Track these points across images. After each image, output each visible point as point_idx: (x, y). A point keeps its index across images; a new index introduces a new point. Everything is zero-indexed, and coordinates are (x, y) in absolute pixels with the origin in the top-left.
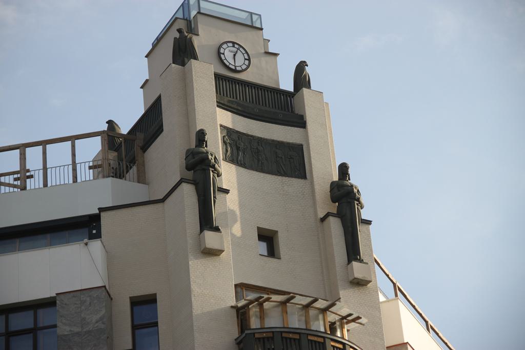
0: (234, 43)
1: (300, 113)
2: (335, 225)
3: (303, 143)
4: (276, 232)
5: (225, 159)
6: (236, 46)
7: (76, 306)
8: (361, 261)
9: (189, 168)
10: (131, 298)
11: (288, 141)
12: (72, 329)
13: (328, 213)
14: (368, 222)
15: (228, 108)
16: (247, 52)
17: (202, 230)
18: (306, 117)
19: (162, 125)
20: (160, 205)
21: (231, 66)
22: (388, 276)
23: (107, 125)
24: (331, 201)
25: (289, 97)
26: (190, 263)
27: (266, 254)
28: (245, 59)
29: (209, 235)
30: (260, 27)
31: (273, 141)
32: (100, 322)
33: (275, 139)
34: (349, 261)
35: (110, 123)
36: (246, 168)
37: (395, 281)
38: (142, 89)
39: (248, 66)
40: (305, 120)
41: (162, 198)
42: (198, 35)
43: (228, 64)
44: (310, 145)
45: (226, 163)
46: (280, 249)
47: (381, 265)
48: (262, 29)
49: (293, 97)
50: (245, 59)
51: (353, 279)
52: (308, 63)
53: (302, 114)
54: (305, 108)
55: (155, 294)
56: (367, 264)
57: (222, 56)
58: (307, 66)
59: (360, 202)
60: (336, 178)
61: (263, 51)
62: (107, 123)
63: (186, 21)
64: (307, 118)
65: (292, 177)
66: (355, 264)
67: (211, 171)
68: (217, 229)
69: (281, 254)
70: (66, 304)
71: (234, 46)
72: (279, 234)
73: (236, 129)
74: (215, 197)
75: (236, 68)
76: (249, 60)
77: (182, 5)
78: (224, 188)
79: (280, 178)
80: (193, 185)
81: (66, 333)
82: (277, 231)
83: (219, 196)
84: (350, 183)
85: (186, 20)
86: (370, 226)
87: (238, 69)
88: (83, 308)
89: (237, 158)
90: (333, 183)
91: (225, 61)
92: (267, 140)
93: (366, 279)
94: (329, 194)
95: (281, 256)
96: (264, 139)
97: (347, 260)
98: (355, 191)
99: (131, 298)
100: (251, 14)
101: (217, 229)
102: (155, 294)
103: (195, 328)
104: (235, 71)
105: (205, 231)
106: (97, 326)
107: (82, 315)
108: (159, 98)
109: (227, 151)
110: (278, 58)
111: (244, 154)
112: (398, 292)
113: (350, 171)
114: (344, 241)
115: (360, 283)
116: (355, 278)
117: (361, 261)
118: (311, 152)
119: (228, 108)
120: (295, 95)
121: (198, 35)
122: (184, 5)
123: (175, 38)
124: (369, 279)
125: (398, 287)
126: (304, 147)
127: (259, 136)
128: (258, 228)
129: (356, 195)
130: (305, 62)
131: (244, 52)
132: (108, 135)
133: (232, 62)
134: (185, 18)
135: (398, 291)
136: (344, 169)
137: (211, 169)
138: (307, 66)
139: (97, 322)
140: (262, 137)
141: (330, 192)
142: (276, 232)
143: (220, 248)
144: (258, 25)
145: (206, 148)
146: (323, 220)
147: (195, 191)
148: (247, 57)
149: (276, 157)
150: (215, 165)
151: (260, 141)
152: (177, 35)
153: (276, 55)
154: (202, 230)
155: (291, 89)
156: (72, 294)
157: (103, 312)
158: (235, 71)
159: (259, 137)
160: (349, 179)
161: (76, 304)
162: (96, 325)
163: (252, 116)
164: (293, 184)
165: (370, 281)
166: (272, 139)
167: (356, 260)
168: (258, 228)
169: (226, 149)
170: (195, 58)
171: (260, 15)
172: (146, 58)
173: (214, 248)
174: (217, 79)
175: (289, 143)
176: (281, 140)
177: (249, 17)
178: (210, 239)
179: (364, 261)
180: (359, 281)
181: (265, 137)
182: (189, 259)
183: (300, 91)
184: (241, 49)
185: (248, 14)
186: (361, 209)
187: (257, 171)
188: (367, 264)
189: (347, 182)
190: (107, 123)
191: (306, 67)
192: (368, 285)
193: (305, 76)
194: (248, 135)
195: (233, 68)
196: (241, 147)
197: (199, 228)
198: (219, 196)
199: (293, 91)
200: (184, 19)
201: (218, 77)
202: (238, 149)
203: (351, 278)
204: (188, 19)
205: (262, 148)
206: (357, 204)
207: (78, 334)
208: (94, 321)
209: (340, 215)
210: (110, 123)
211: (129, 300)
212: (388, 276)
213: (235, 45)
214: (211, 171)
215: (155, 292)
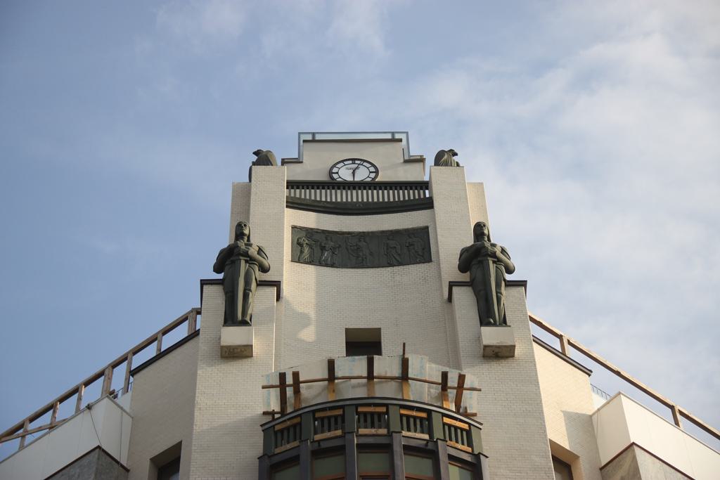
2: (465, 299)
9: (218, 269)
14: (523, 284)
15: (309, 208)
16: (373, 165)
22: (618, 373)
24: (459, 272)
26: (199, 372)
31: (383, 232)
37: (671, 403)
47: (622, 373)
56: (510, 326)
58: (456, 154)
61: (402, 161)
92: (372, 233)
96: (368, 233)
112: (679, 416)
114: (477, 311)
115: (500, 354)
119: (309, 208)
125: (681, 413)
126: (429, 229)
127: (361, 231)
131: (368, 165)
135: (679, 416)
136: (480, 231)
138: (456, 154)
149: (387, 249)
151: (362, 236)
156: (61, 473)
159: (360, 233)
163: (350, 212)
166: (381, 229)
167: (489, 324)
180: (497, 350)
181: (370, 230)
182: (199, 368)
184: (365, 164)
188: (510, 326)
191: (455, 158)
194: (343, 233)
196: (327, 246)
205: (365, 244)
212: (618, 373)
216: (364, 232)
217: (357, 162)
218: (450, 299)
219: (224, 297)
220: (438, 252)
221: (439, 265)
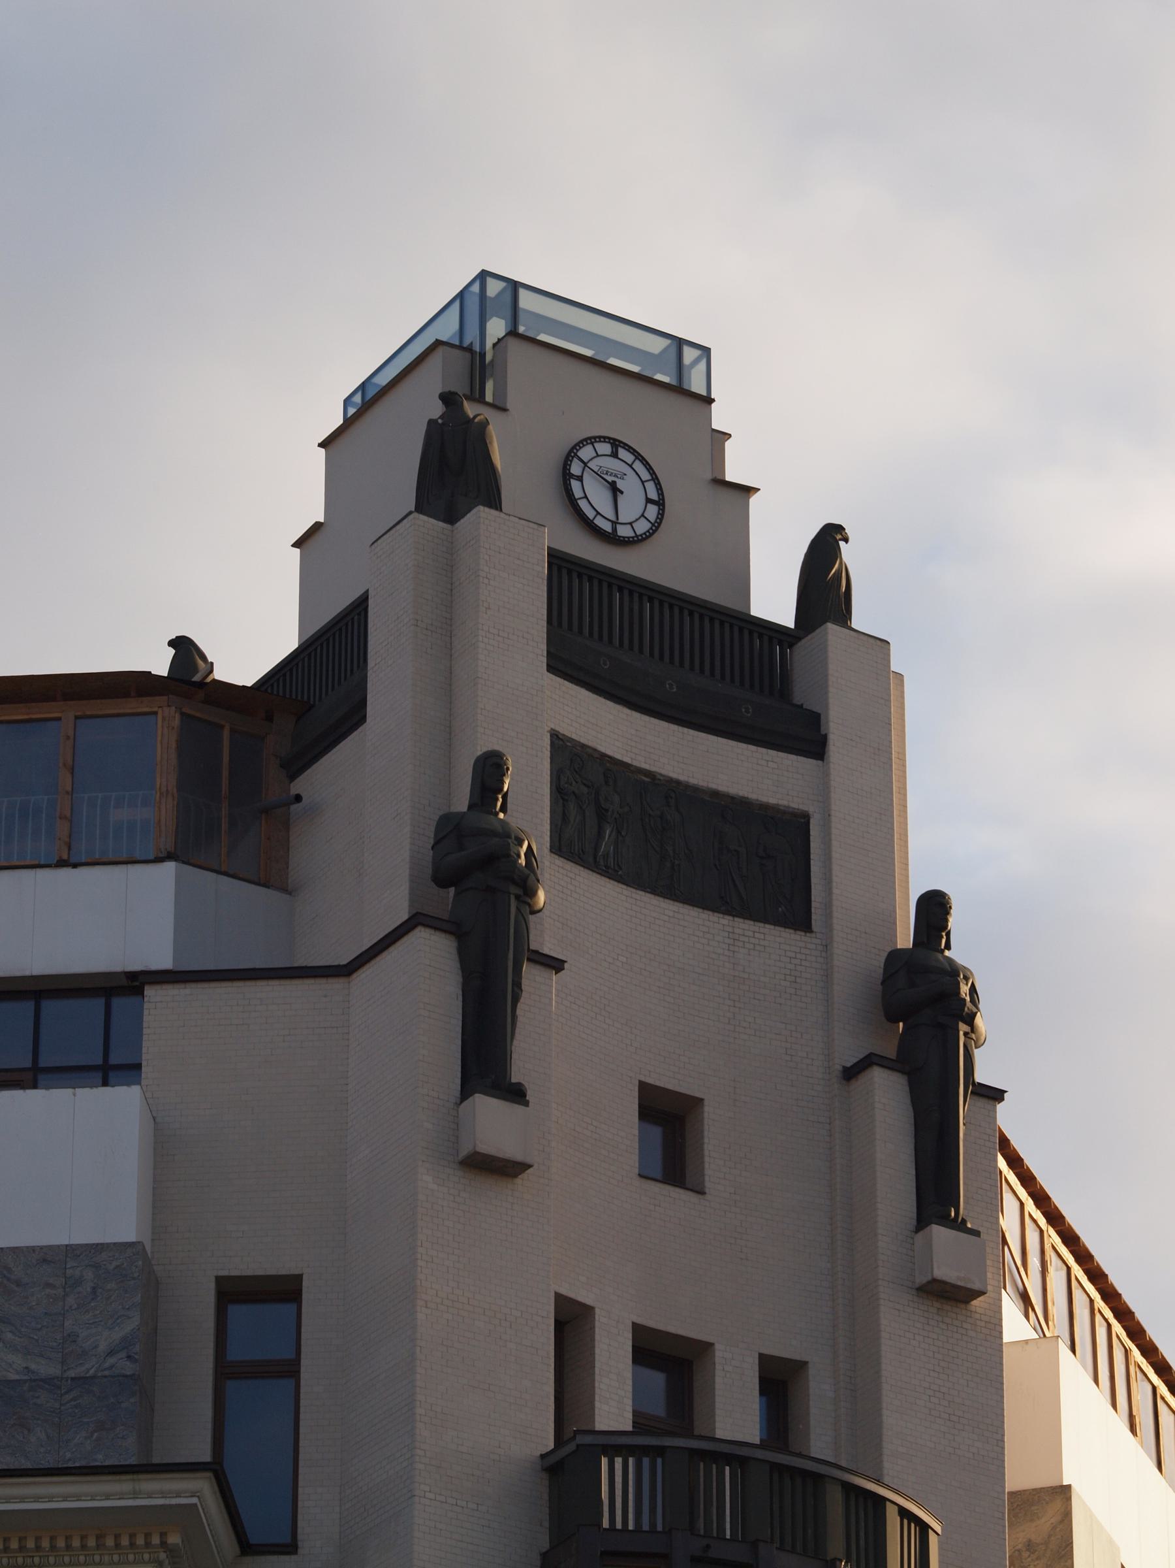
0: (616, 444)
1: (811, 705)
3: (811, 809)
4: (697, 1102)
5: (560, 847)
7: (48, 1291)
8: (959, 1225)
9: (442, 879)
10: (219, 1280)
11: (764, 799)
12: (33, 1366)
13: (871, 1054)
17: (466, 1092)
18: (827, 722)
19: (363, 703)
20: (334, 985)
21: (599, 522)
23: (172, 651)
25: (780, 643)
27: (659, 1177)
28: (649, 501)
30: (704, 393)
31: (716, 794)
32: (123, 1354)
33: (722, 788)
34: (922, 1222)
35: (183, 647)
36: (620, 880)
38: (298, 551)
39: (656, 526)
40: (823, 732)
41: (344, 962)
43: (590, 514)
44: (833, 819)
45: (559, 861)
46: (707, 1159)
48: (709, 400)
49: (791, 646)
50: (649, 501)
51: (929, 1282)
52: (849, 531)
53: (816, 709)
54: (827, 693)
55: (299, 1278)
56: (976, 1233)
57: (575, 484)
58: (846, 540)
59: (973, 1028)
60: (905, 938)
61: (709, 476)
62: (172, 643)
63: (468, 355)
64: (831, 724)
65: (765, 920)
66: (938, 1232)
67: (512, 898)
68: (517, 1094)
69: (707, 1178)
70: (18, 1283)
71: (615, 455)
72: (706, 1109)
73: (603, 750)
74: (517, 985)
75: (615, 530)
76: (660, 503)
77: (461, 295)
78: (546, 951)
79: (726, 920)
80: (448, 936)
81: (13, 1376)
82: (702, 1100)
83: (531, 975)
84: (949, 960)
85: (469, 349)
86: (1000, 1107)
87: (624, 532)
88: (71, 1301)
89: (596, 848)
90: (895, 957)
91: (583, 504)
92: (696, 789)
93: (969, 1286)
94: (880, 988)
95: (707, 1184)
96: (687, 786)
97: (915, 1216)
98: (965, 989)
99: (219, 1280)
100: (680, 343)
101: (517, 1094)
102: (299, 1278)
103: (419, 1411)
104: (611, 539)
105: (477, 1095)
106: (111, 1367)
107: (67, 1324)
108: (360, 607)
109: (565, 818)
110: (754, 500)
111: (619, 832)
113: (952, 922)
116: (934, 1281)
117: (959, 1225)
118: (835, 843)
120: (799, 639)
122: (467, 295)
123: (431, 423)
124: (976, 1286)
126: (812, 821)
127: (674, 776)
128: (640, 1082)
129: (965, 1004)
130: (839, 528)
131: (645, 475)
132: (183, 714)
133: (607, 510)
134: (466, 344)
137: (514, 890)
138: (846, 540)
139: (111, 1353)
140: (682, 778)
141: (883, 983)
142: (697, 1102)
143: (519, 1157)
144: (698, 387)
145: (501, 815)
146: (850, 1074)
147: (455, 956)
148: (653, 495)
150: (528, 877)
153: (748, 491)
154: (466, 1092)
155: (790, 622)
157: (133, 1323)
158: (611, 539)
159: (670, 780)
160: (948, 947)
161: (48, 1285)
162: (111, 1361)
165: (982, 1293)
166: (713, 786)
168: (640, 1082)
169: (564, 813)
170: (493, 500)
171: (706, 351)
172: (323, 451)
173: (501, 1155)
174: (555, 569)
175: (765, 807)
176: (741, 793)
177: (673, 350)
179: (969, 1225)
181: (693, 781)
183: (823, 627)
184: (638, 466)
185: (667, 342)
186: (976, 1048)
187: (654, 891)
188: (976, 1233)
189: (940, 956)
190: (172, 643)
191: (842, 544)
192: (974, 1303)
193: (838, 574)
195: (607, 527)
197: (458, 1081)
198: (531, 975)
199: (792, 625)
200: (460, 347)
201: (559, 563)
202: (601, 815)
203: (921, 1279)
204: (477, 348)
206: (966, 1034)
207: (49, 1383)
208: (103, 1346)
209: (903, 1063)
210: (183, 647)
211: (212, 1285)
214: (512, 898)
215: (297, 1272)
216: (678, 782)
217: (622, 453)
218: (850, 1074)
219: (461, 980)
220: (828, 906)
221: (827, 947)
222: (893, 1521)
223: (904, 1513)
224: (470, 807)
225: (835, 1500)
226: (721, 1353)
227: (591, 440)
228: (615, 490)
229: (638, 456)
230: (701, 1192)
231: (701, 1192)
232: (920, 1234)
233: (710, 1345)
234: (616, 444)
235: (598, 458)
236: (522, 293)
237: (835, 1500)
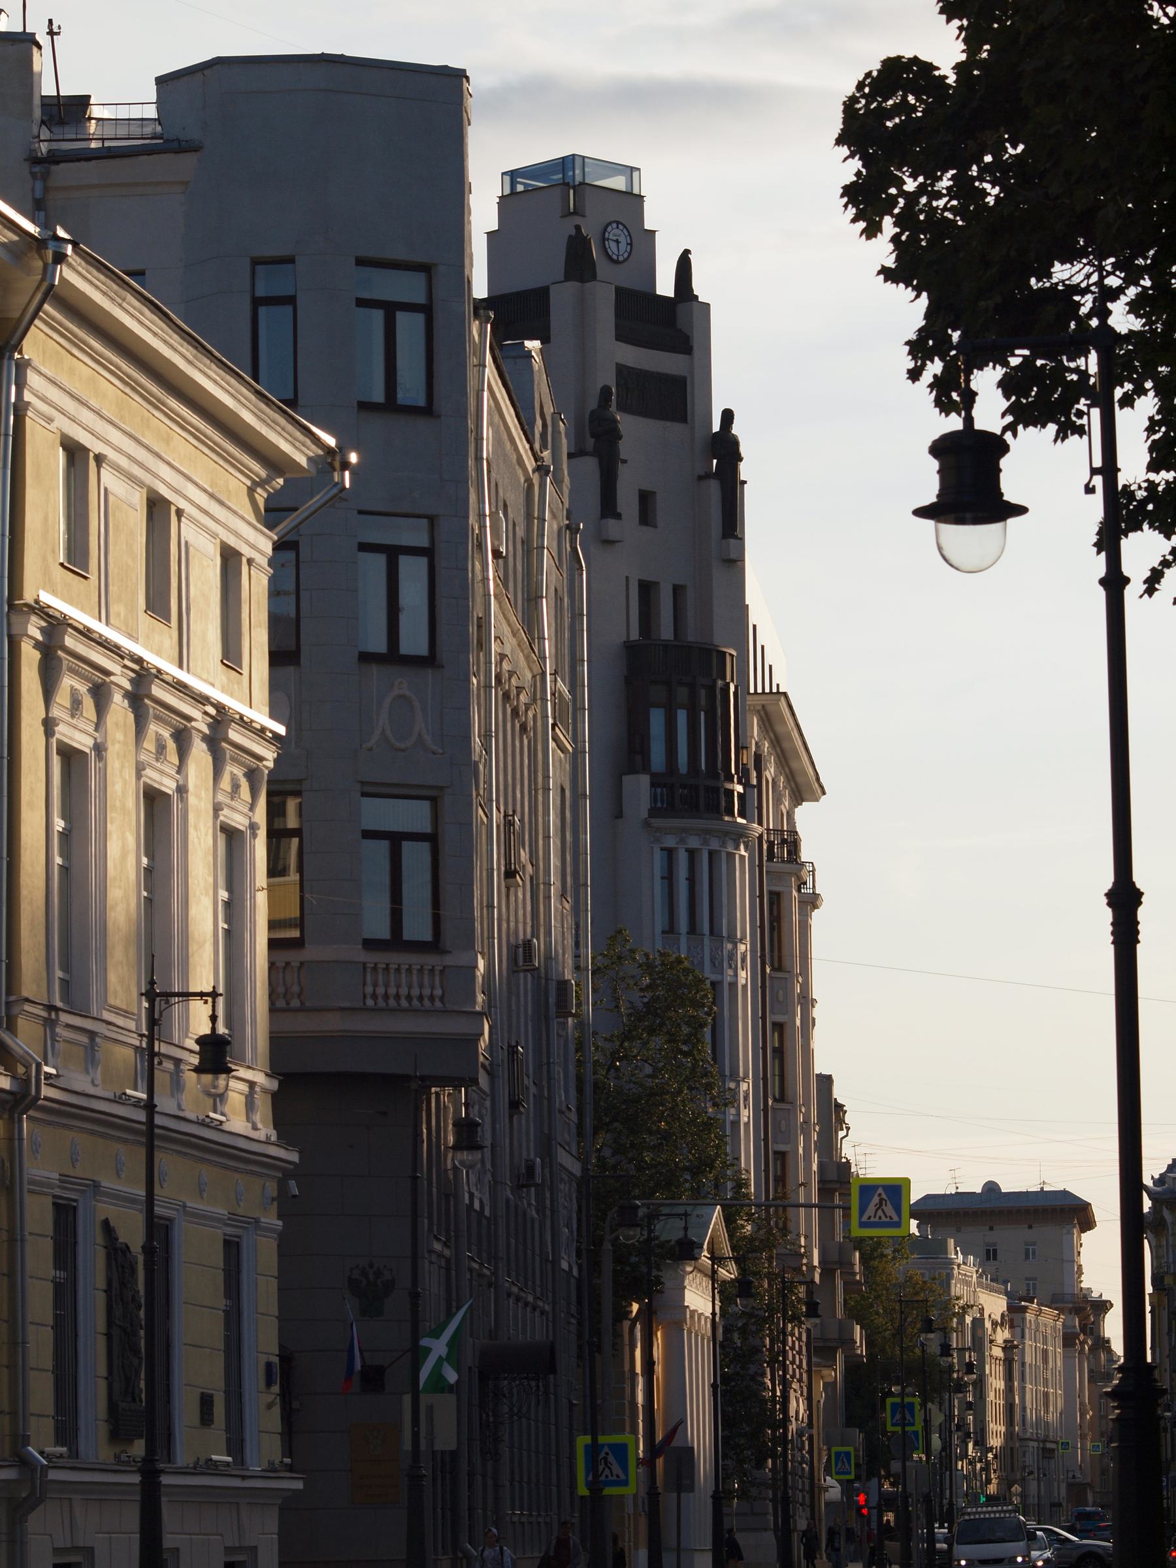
2: (714, 487)
6: (621, 227)
8: (736, 538)
16: (630, 235)
29: (611, 522)
42: (584, 216)
43: (610, 253)
66: (732, 541)
76: (631, 244)
79: (662, 422)
91: (609, 250)
92: (653, 373)
104: (617, 262)
117: (736, 538)
121: (584, 216)
136: (728, 416)
146: (700, 478)
152: (573, 232)
158: (617, 262)
164: (675, 429)
170: (594, 277)
178: (612, 527)
195: (615, 257)
204: (571, 184)
213: (620, 226)
218: (700, 478)
222: (728, 656)
223: (730, 654)
224: (599, 406)
225: (715, 655)
226: (662, 585)
227: (610, 224)
228: (617, 242)
229: (625, 227)
230: (655, 526)
231: (655, 526)
232: (724, 541)
233: (657, 583)
234: (618, 223)
235: (613, 233)
236: (586, 160)
237: (715, 655)
